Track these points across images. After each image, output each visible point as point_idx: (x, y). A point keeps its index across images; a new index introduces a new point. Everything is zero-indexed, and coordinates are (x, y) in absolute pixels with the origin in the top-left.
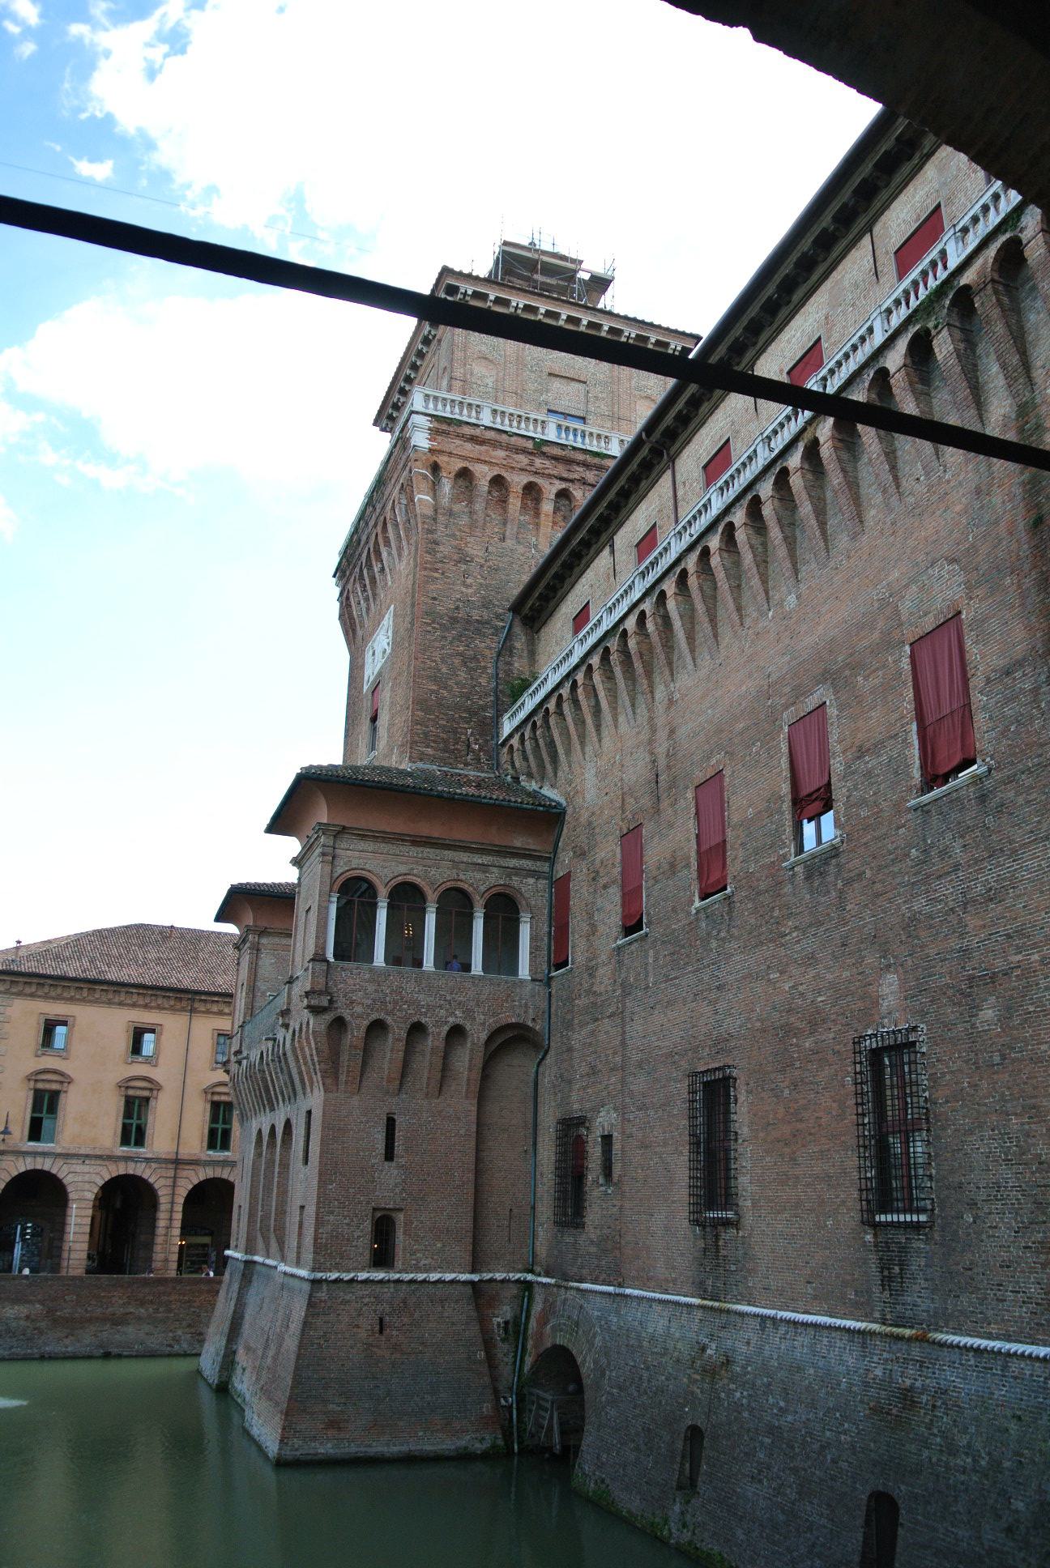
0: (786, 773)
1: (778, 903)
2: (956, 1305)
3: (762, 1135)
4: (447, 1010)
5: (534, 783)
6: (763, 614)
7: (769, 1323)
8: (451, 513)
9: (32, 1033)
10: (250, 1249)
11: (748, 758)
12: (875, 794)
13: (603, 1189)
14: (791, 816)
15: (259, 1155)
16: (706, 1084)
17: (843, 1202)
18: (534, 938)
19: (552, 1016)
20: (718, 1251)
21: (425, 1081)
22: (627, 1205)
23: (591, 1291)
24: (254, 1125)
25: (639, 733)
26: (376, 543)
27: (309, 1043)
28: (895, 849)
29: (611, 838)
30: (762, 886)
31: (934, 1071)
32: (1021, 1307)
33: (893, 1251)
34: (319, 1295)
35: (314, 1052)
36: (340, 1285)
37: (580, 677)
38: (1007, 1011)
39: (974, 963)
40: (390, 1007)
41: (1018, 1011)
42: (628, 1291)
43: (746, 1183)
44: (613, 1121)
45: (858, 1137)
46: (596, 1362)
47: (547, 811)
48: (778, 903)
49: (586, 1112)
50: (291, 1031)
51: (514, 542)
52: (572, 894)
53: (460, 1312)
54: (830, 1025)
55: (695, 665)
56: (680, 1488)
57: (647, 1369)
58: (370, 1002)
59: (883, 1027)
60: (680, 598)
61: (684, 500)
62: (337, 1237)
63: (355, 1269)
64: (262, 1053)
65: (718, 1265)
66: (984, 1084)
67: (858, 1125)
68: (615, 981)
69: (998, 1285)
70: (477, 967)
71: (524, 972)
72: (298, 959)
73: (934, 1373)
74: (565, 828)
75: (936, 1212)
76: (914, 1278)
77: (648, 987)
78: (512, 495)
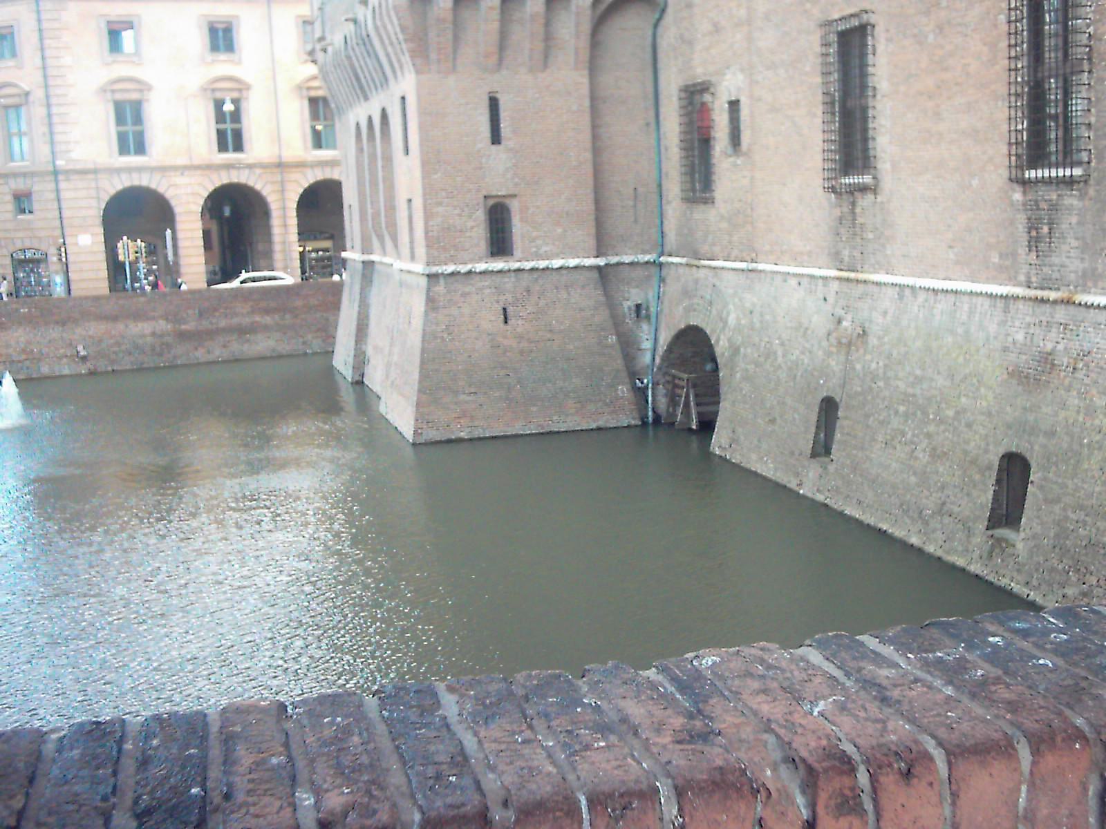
3: (902, 88)
7: (907, 292)
9: (96, 40)
10: (366, 250)
13: (732, 159)
15: (360, 150)
16: (843, 35)
20: (854, 219)
35: (398, 30)
36: (458, 277)
42: (760, 266)
46: (729, 340)
50: (370, 7)
53: (586, 298)
56: (814, 455)
63: (471, 261)
65: (855, 234)
75: (1093, 164)
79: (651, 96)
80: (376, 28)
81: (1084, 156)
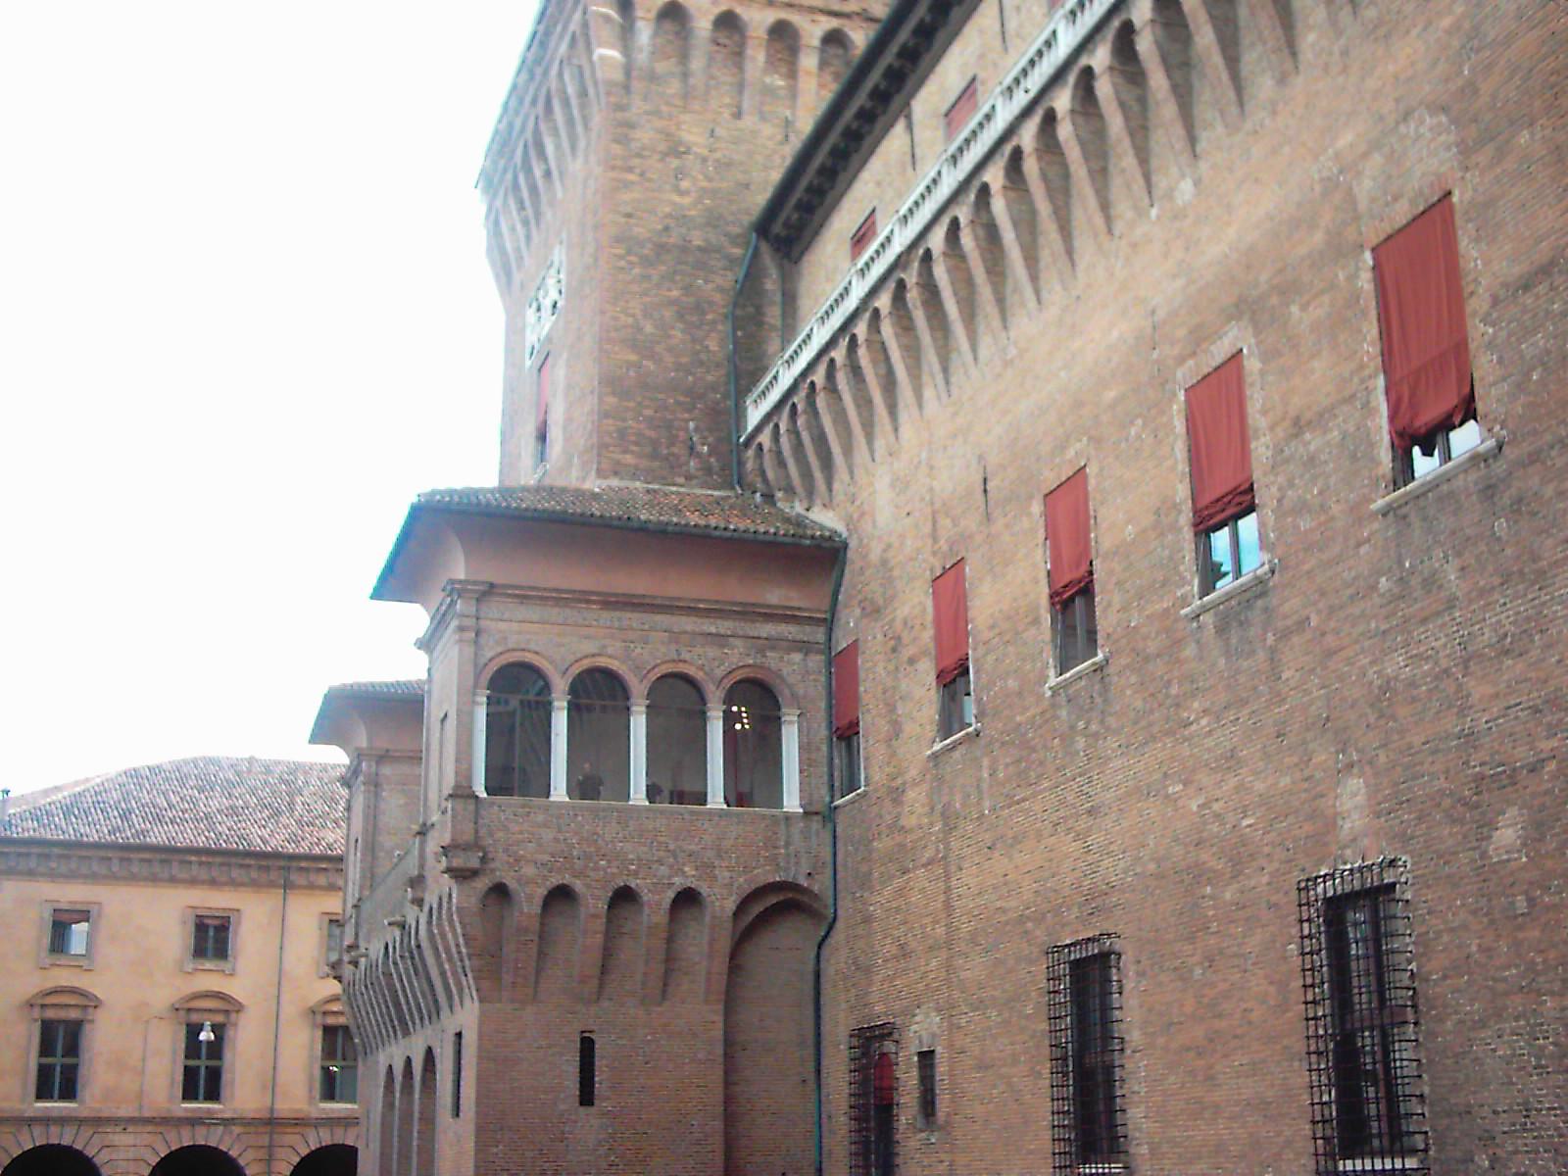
0: (1183, 467)
1: (1176, 673)
3: (1161, 1041)
4: (671, 867)
5: (797, 504)
6: (1141, 213)
8: (652, 77)
9: (33, 931)
11: (1123, 445)
12: (1321, 493)
13: (924, 1135)
15: (389, 1105)
16: (1076, 965)
17: (1289, 1143)
18: (804, 748)
19: (839, 868)
21: (639, 977)
24: (382, 1059)
25: (955, 414)
26: (537, 132)
28: (1355, 578)
30: (1152, 647)
35: (461, 940)
37: (861, 329)
39: (1483, 755)
40: (578, 864)
41: (1553, 828)
43: (1138, 1118)
44: (935, 1029)
45: (1308, 1038)
48: (1176, 673)
50: (426, 909)
51: (756, 119)
52: (862, 675)
54: (1262, 862)
55: (1039, 301)
58: (546, 858)
59: (1345, 863)
60: (1012, 194)
61: (1018, 35)
67: (1307, 1019)
68: (932, 809)
70: (716, 799)
71: (792, 802)
72: (433, 796)
74: (847, 571)
75: (1431, 1153)
78: (750, 43)
80: (431, 936)
81: (1419, 1141)
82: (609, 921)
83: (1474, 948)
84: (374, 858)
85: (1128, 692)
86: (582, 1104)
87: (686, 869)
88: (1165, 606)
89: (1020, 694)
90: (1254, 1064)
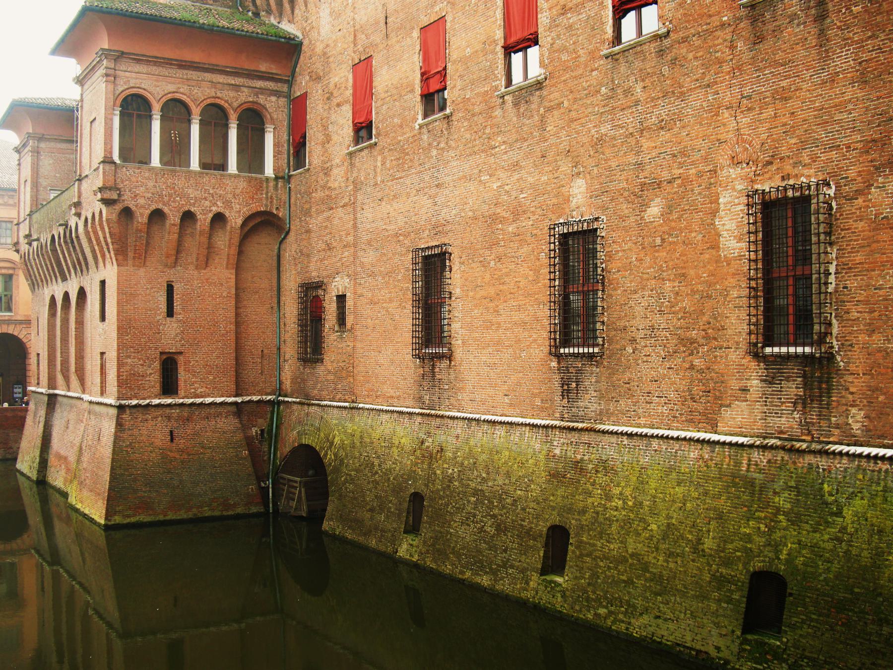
0: (500, 22)
1: (489, 123)
2: (616, 407)
3: (471, 294)
4: (211, 201)
10: (52, 384)
11: (467, 8)
12: (574, 43)
14: (503, 56)
16: (426, 258)
18: (276, 145)
20: (434, 376)
21: (195, 256)
22: (359, 345)
23: (330, 406)
24: (47, 292)
27: (102, 229)
28: (588, 86)
29: (344, 66)
31: (610, 249)
32: (663, 406)
33: (572, 373)
34: (123, 416)
35: (108, 235)
36: (140, 409)
38: (669, 209)
39: (646, 173)
40: (166, 199)
41: (677, 208)
42: (361, 405)
44: (347, 284)
46: (336, 455)
47: (288, 43)
48: (489, 123)
49: (323, 278)
50: (83, 218)
53: (228, 424)
54: (529, 215)
57: (378, 457)
58: (150, 195)
59: (572, 218)
62: (134, 374)
63: (149, 397)
64: (53, 237)
66: (648, 259)
67: (550, 287)
69: (648, 393)
71: (269, 171)
73: (598, 451)
74: (301, 56)
75: (606, 346)
76: (587, 390)
77: (376, 184)
79: (275, 289)
80: (87, 233)
81: (600, 341)
82: (180, 228)
83: (634, 259)
84: (37, 191)
85: (463, 130)
86: (168, 316)
87: (218, 203)
88: (486, 89)
89: (401, 126)
90: (520, 306)
